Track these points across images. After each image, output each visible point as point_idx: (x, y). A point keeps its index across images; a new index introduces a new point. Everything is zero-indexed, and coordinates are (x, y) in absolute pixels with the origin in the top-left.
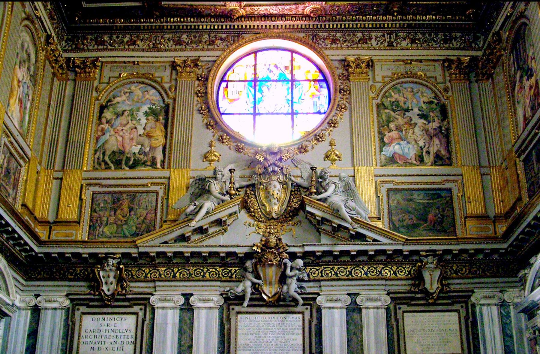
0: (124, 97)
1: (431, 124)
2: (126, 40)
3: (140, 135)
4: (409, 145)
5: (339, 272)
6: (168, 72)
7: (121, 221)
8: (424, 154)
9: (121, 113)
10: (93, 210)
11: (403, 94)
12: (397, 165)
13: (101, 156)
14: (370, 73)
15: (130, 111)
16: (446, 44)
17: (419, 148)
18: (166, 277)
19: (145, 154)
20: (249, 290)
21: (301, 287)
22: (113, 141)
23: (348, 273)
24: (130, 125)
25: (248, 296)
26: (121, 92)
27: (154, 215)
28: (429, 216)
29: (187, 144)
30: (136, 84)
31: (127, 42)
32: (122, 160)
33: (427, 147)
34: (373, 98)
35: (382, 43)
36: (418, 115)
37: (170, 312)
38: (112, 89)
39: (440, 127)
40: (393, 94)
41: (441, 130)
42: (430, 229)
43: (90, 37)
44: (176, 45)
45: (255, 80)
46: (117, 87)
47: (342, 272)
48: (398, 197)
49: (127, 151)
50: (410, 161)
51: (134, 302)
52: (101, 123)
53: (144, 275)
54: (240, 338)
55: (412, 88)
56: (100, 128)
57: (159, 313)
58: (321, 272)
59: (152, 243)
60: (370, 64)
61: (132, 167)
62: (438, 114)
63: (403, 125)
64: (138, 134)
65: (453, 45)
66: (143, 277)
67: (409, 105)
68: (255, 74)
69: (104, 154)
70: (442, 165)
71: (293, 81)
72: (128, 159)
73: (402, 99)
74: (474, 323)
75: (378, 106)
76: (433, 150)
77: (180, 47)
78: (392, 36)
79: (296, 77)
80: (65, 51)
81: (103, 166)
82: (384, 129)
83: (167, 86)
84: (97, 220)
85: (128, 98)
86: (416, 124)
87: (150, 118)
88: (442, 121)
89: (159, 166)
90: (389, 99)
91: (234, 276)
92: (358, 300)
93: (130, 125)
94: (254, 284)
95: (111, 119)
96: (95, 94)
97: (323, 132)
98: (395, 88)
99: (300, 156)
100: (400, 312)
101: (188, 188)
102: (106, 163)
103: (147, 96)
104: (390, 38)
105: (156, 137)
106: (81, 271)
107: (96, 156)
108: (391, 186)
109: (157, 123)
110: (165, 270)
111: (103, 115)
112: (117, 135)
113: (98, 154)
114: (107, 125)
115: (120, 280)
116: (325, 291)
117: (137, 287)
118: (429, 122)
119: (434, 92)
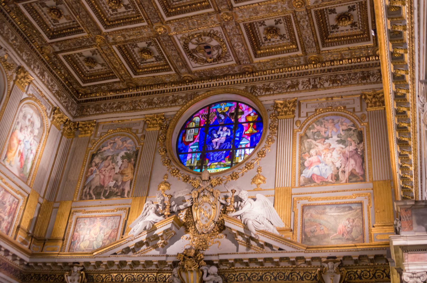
0: (109, 147)
1: (348, 147)
2: (115, 106)
3: (116, 174)
4: (327, 167)
5: (252, 277)
7: (93, 238)
8: (340, 173)
9: (105, 158)
10: (75, 230)
11: (325, 125)
12: (315, 184)
13: (88, 190)
14: (297, 111)
15: (112, 156)
16: (363, 80)
17: (335, 169)
18: (116, 281)
23: (259, 278)
24: (111, 166)
26: (107, 143)
27: (116, 233)
28: (339, 227)
30: (119, 137)
31: (116, 107)
32: (101, 192)
33: (343, 166)
34: (298, 131)
35: (308, 86)
36: (337, 141)
38: (102, 141)
39: (356, 149)
40: (315, 126)
41: (357, 152)
42: (340, 239)
44: (149, 106)
46: (105, 140)
47: (255, 277)
49: (106, 185)
50: (327, 180)
53: (101, 279)
55: (333, 120)
56: (90, 170)
58: (237, 278)
59: (105, 254)
61: (107, 198)
62: (355, 138)
63: (323, 150)
64: (115, 172)
65: (370, 80)
66: (100, 281)
68: (208, 121)
69: (90, 189)
70: (356, 181)
72: (106, 191)
75: (301, 137)
76: (348, 169)
77: (152, 107)
78: (316, 80)
81: (88, 197)
82: (305, 156)
83: (139, 135)
84: (77, 238)
85: (112, 147)
86: (334, 149)
87: (125, 160)
88: (358, 144)
89: (126, 195)
90: (311, 131)
91: (167, 281)
93: (111, 166)
95: (98, 163)
97: (252, 161)
98: (318, 121)
102: (90, 196)
103: (125, 145)
104: (315, 81)
105: (127, 174)
106: (59, 276)
107: (85, 190)
109: (130, 164)
110: (117, 276)
111: (94, 160)
112: (101, 174)
113: (86, 188)
114: (95, 167)
118: (346, 146)
119: (352, 121)
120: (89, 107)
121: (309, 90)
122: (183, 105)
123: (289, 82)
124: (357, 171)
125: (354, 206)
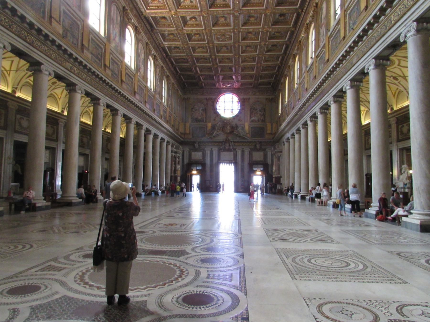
57: (206, 152)
60: (249, 99)
74: (266, 154)
76: (262, 118)
94: (224, 147)
96: (190, 106)
101: (211, 127)
108: (252, 127)
115: (199, 145)
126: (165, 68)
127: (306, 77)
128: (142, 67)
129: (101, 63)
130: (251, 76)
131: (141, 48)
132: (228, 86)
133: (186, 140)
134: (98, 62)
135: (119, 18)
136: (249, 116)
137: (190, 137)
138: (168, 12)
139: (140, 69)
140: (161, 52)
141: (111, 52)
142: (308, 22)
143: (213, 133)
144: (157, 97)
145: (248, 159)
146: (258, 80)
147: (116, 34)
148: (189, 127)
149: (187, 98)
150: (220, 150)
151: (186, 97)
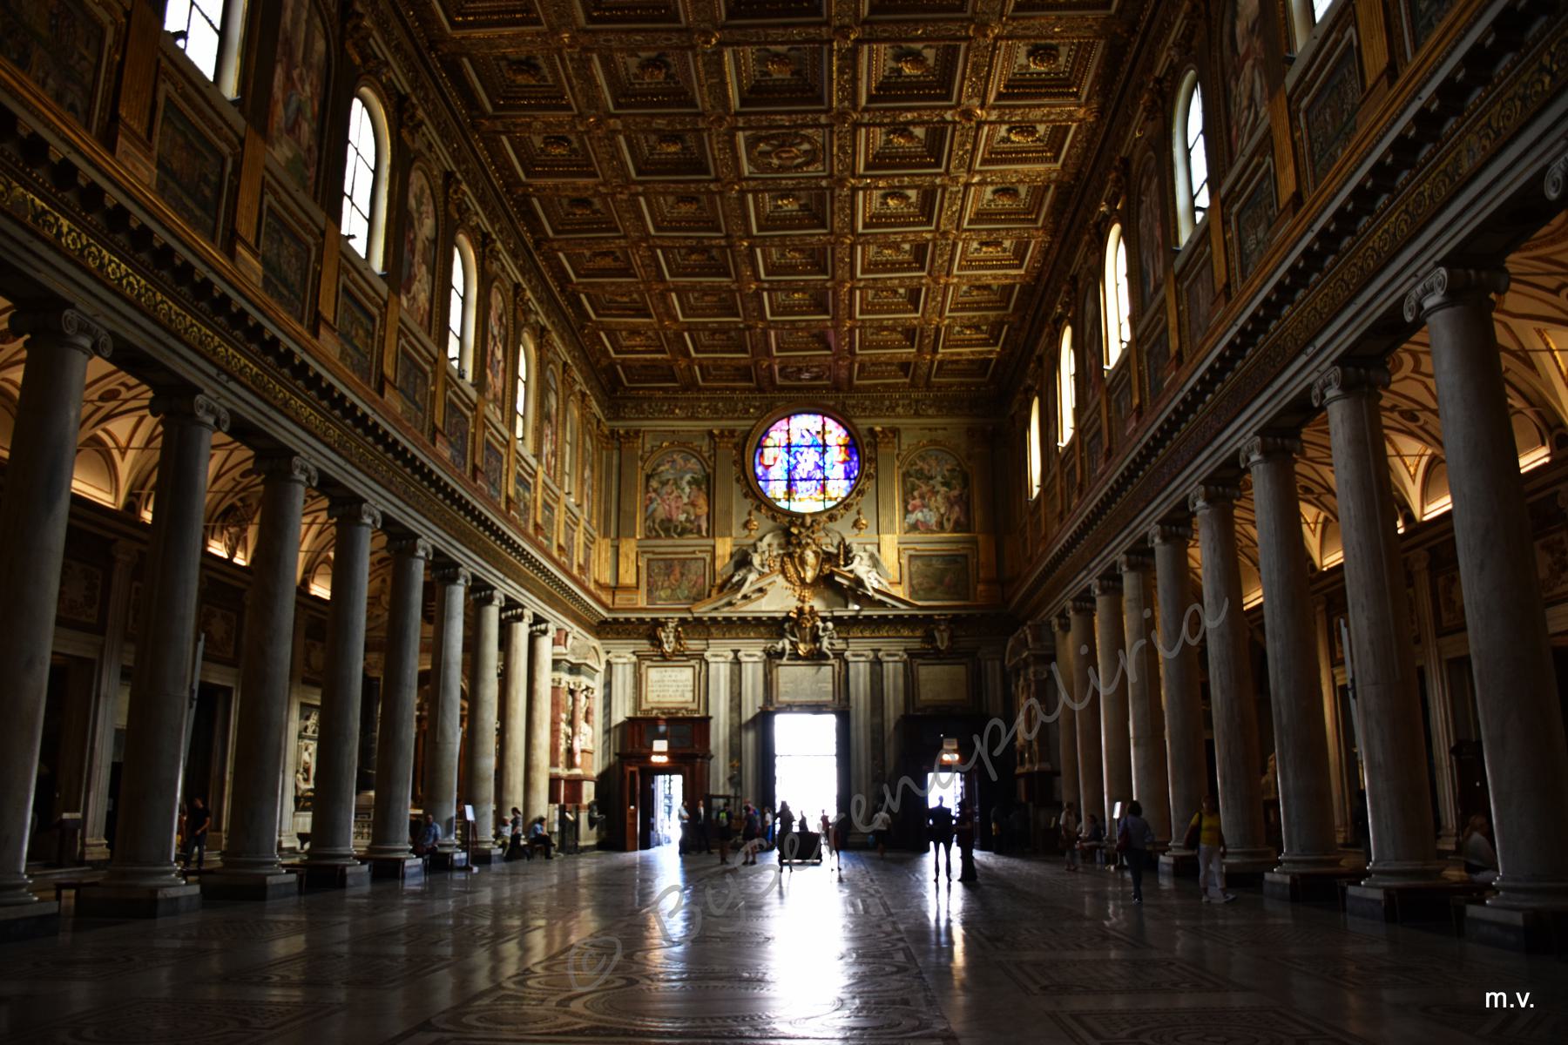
0: (667, 466)
2: (665, 408)
6: (707, 440)
19: (691, 522)
20: (788, 647)
21: (832, 644)
22: (660, 509)
24: (675, 494)
25: (788, 652)
29: (728, 514)
37: (722, 665)
43: (629, 405)
45: (789, 446)
48: (918, 563)
49: (674, 517)
51: (691, 657)
52: (648, 492)
54: (781, 685)
57: (712, 667)
60: (895, 432)
61: (680, 535)
67: (933, 473)
71: (825, 446)
72: (676, 527)
73: (926, 467)
76: (954, 517)
79: (828, 442)
80: (608, 419)
83: (706, 455)
86: (938, 492)
92: (880, 654)
93: (675, 494)
96: (640, 464)
99: (830, 525)
100: (915, 665)
101: (732, 556)
115: (678, 638)
116: (852, 646)
117: (694, 645)
120: (626, 407)
121: (911, 417)
122: (758, 419)
123: (887, 403)
124: (962, 519)
125: (959, 559)
126: (529, 294)
127: (1171, 302)
128: (422, 272)
129: (210, 222)
130: (910, 334)
131: (422, 190)
132: (806, 376)
133: (621, 616)
134: (198, 212)
135: (320, 45)
136: (897, 504)
137: (641, 600)
138: (545, 34)
139: (411, 278)
140: (511, 221)
141: (268, 177)
142: (1159, 71)
143: (744, 580)
144: (493, 413)
145: (901, 696)
146: (935, 351)
147: (299, 110)
148: (633, 556)
149: (627, 432)
150: (772, 657)
151: (621, 426)
